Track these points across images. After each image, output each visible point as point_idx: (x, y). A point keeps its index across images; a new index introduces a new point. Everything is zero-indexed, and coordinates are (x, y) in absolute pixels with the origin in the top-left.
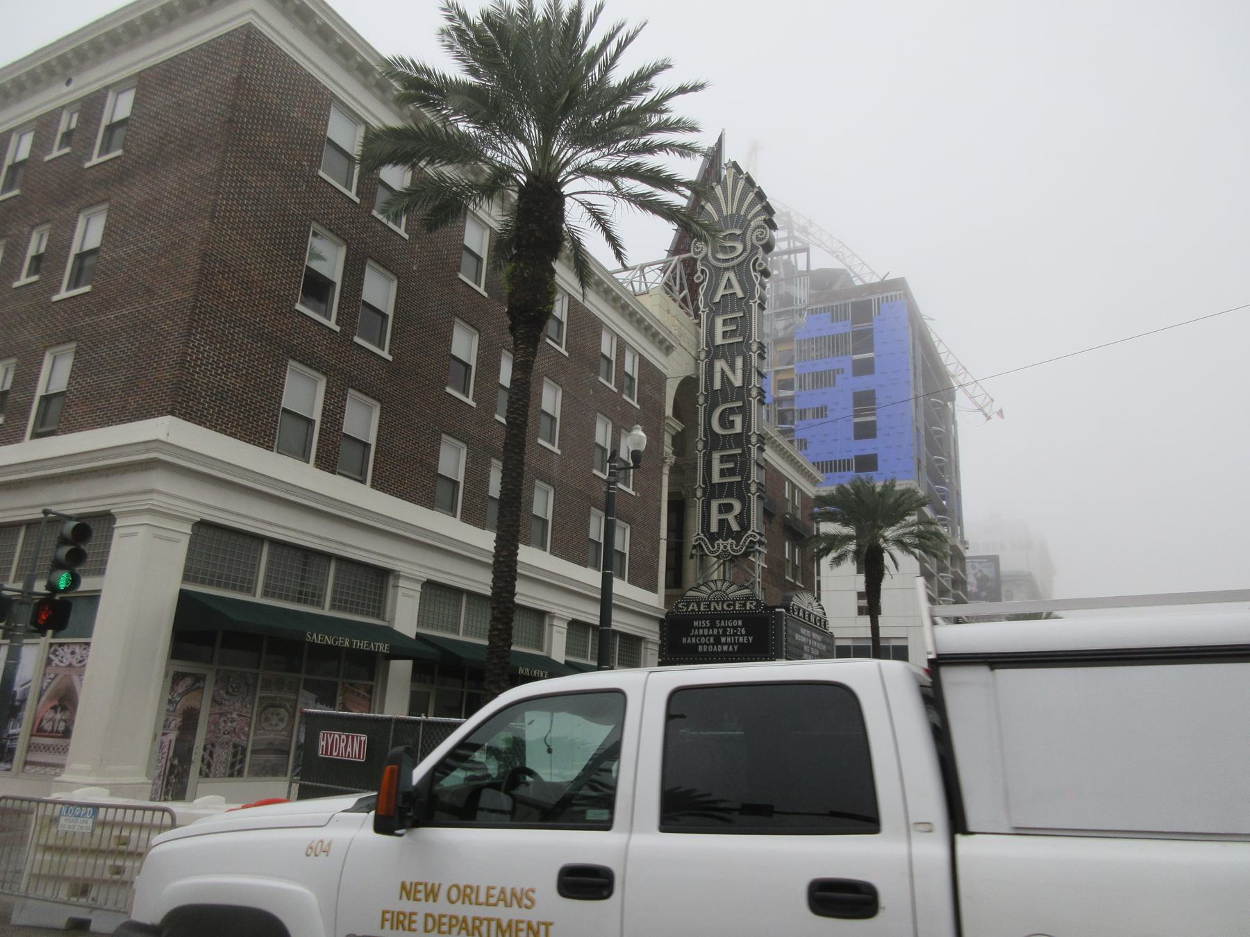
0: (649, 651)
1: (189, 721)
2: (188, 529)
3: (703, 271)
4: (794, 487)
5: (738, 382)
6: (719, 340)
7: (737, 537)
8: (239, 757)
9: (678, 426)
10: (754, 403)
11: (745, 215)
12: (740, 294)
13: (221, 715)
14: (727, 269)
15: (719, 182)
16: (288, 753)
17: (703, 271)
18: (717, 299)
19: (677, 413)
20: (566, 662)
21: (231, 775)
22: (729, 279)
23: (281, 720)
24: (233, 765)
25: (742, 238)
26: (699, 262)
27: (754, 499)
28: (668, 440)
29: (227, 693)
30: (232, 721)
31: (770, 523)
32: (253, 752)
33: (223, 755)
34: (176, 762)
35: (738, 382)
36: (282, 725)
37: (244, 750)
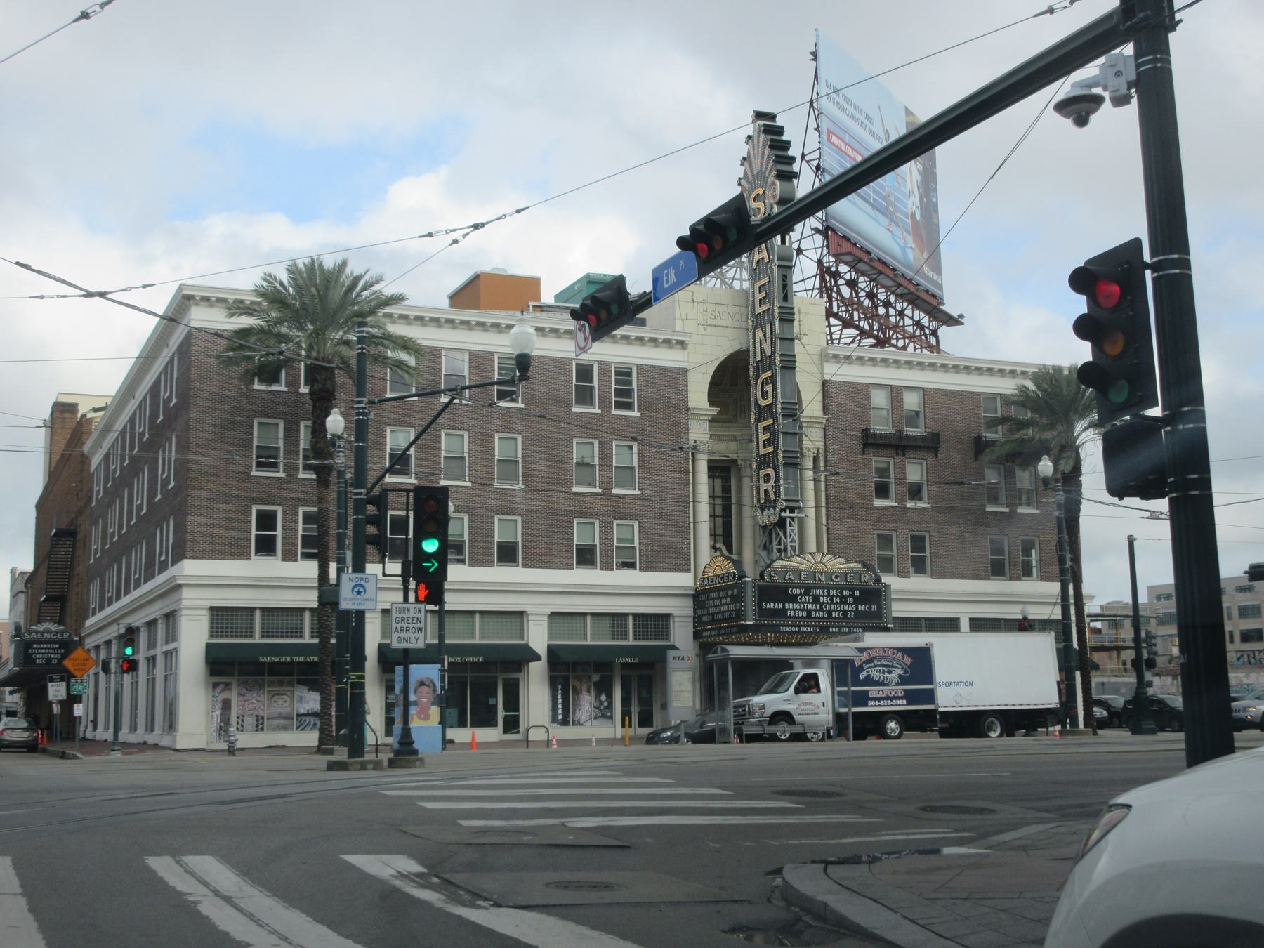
0: (676, 624)
1: (226, 705)
5: (768, 352)
6: (759, 310)
7: (773, 504)
8: (260, 721)
9: (714, 411)
13: (245, 701)
16: (293, 719)
20: (549, 647)
21: (257, 730)
23: (285, 702)
24: (257, 726)
29: (247, 690)
30: (253, 704)
31: (937, 456)
32: (268, 719)
33: (250, 721)
34: (222, 725)
35: (768, 352)
36: (287, 704)
37: (263, 718)
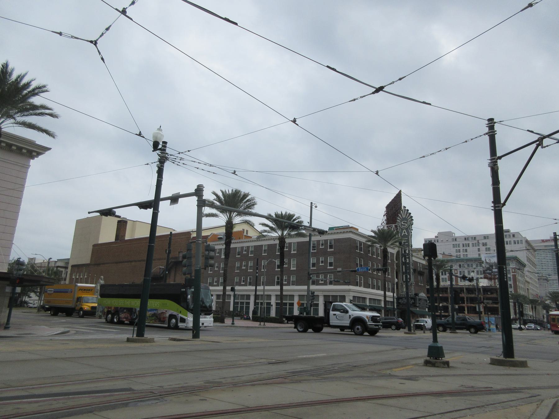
2: (352, 297)
3: (399, 229)
4: (420, 263)
9: (397, 262)
10: (411, 257)
11: (407, 218)
12: (407, 235)
14: (404, 229)
15: (401, 210)
17: (399, 229)
18: (402, 235)
19: (396, 260)
22: (404, 231)
25: (407, 223)
26: (398, 227)
27: (412, 275)
28: (395, 265)
